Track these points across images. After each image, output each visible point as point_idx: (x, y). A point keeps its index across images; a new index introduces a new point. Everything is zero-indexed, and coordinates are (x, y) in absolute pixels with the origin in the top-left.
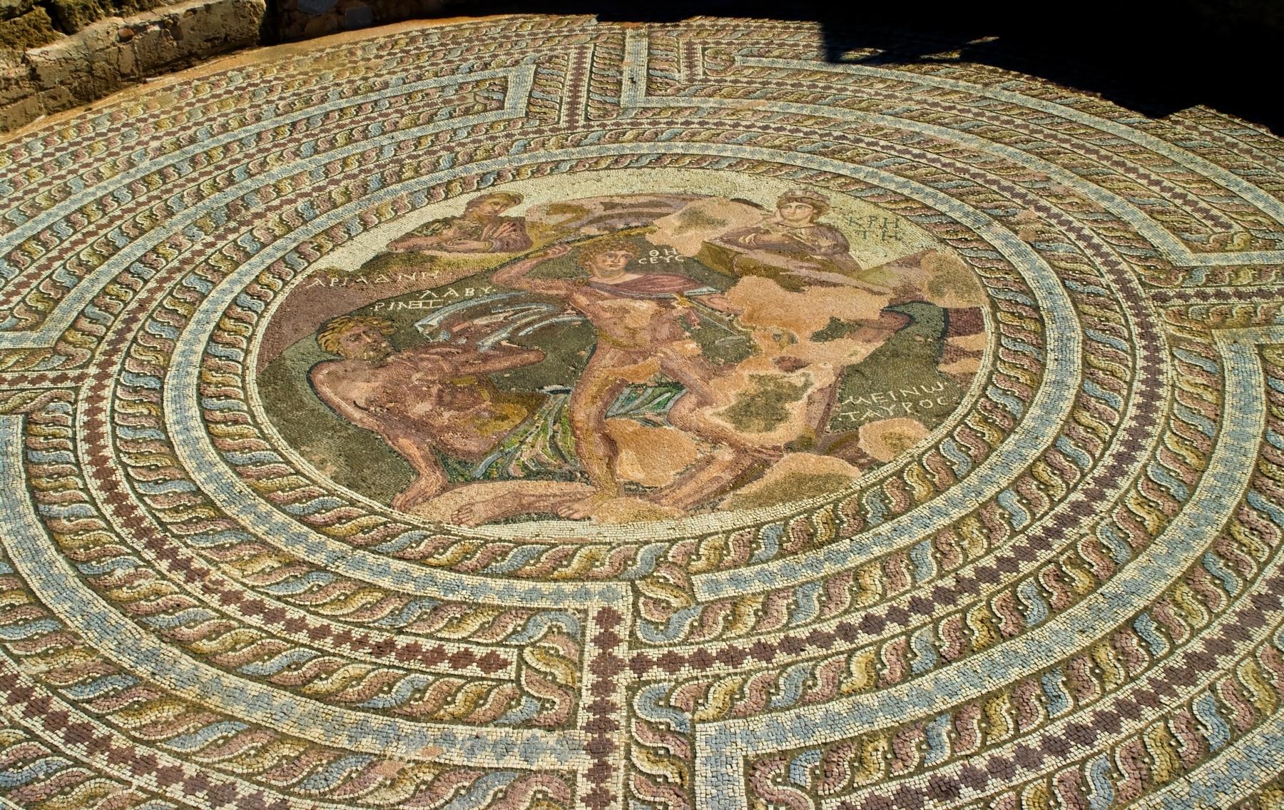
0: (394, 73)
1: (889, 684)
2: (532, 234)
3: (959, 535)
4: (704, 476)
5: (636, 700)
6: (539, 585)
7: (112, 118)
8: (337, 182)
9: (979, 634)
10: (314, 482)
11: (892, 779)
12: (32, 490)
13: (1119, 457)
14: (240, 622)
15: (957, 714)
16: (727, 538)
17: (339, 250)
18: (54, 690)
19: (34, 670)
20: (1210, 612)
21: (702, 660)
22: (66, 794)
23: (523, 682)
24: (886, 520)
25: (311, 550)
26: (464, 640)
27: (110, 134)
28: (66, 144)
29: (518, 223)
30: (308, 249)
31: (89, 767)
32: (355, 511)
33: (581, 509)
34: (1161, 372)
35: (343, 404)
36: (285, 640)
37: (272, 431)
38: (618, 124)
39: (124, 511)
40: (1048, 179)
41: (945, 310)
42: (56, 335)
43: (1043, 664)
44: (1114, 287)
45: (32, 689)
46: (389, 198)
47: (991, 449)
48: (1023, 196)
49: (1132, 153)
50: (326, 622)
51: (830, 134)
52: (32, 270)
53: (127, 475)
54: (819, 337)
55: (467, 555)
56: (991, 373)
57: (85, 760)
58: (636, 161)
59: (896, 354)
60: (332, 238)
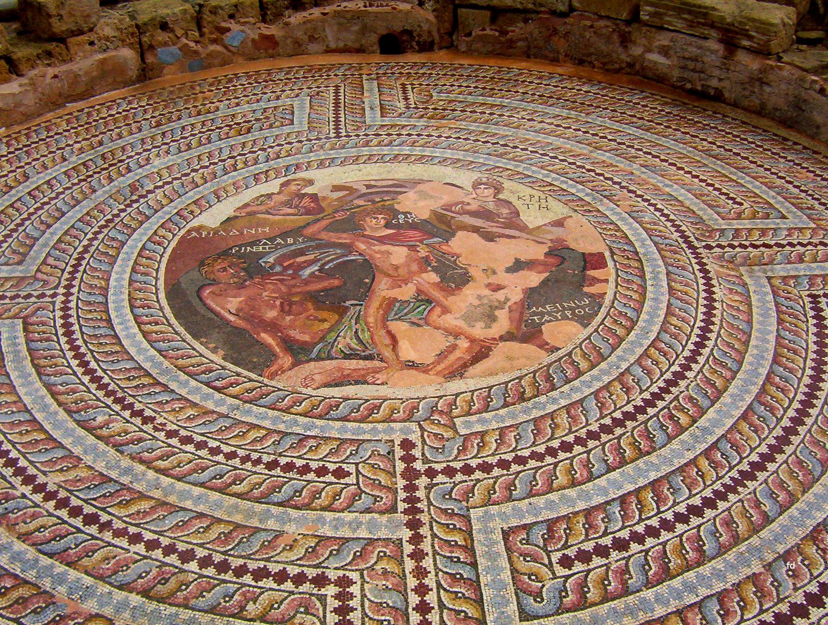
0: (222, 101)
1: (580, 484)
2: (323, 204)
3: (609, 392)
4: (452, 358)
5: (432, 494)
6: (362, 425)
7: (48, 129)
8: (196, 171)
10: (212, 362)
11: (590, 540)
12: (35, 366)
13: (696, 344)
14: (180, 449)
15: (623, 500)
16: (473, 395)
17: (204, 214)
19: (57, 480)
20: (759, 437)
21: (467, 470)
22: (89, 557)
23: (361, 485)
24: (566, 383)
26: (321, 460)
27: (48, 140)
28: (21, 146)
29: (314, 197)
30: (185, 213)
31: (103, 540)
32: (242, 379)
33: (381, 377)
34: (714, 293)
35: (222, 312)
37: (181, 329)
38: (367, 135)
39: (96, 379)
40: (632, 173)
41: (583, 254)
42: (35, 268)
44: (680, 240)
45: (57, 492)
46: (230, 181)
47: (621, 340)
48: (619, 183)
49: (680, 158)
50: (234, 449)
51: (497, 143)
52: (12, 226)
53: (94, 357)
54: (509, 270)
56: (616, 293)
57: (98, 535)
58: (382, 159)
59: (557, 281)
60: (200, 207)
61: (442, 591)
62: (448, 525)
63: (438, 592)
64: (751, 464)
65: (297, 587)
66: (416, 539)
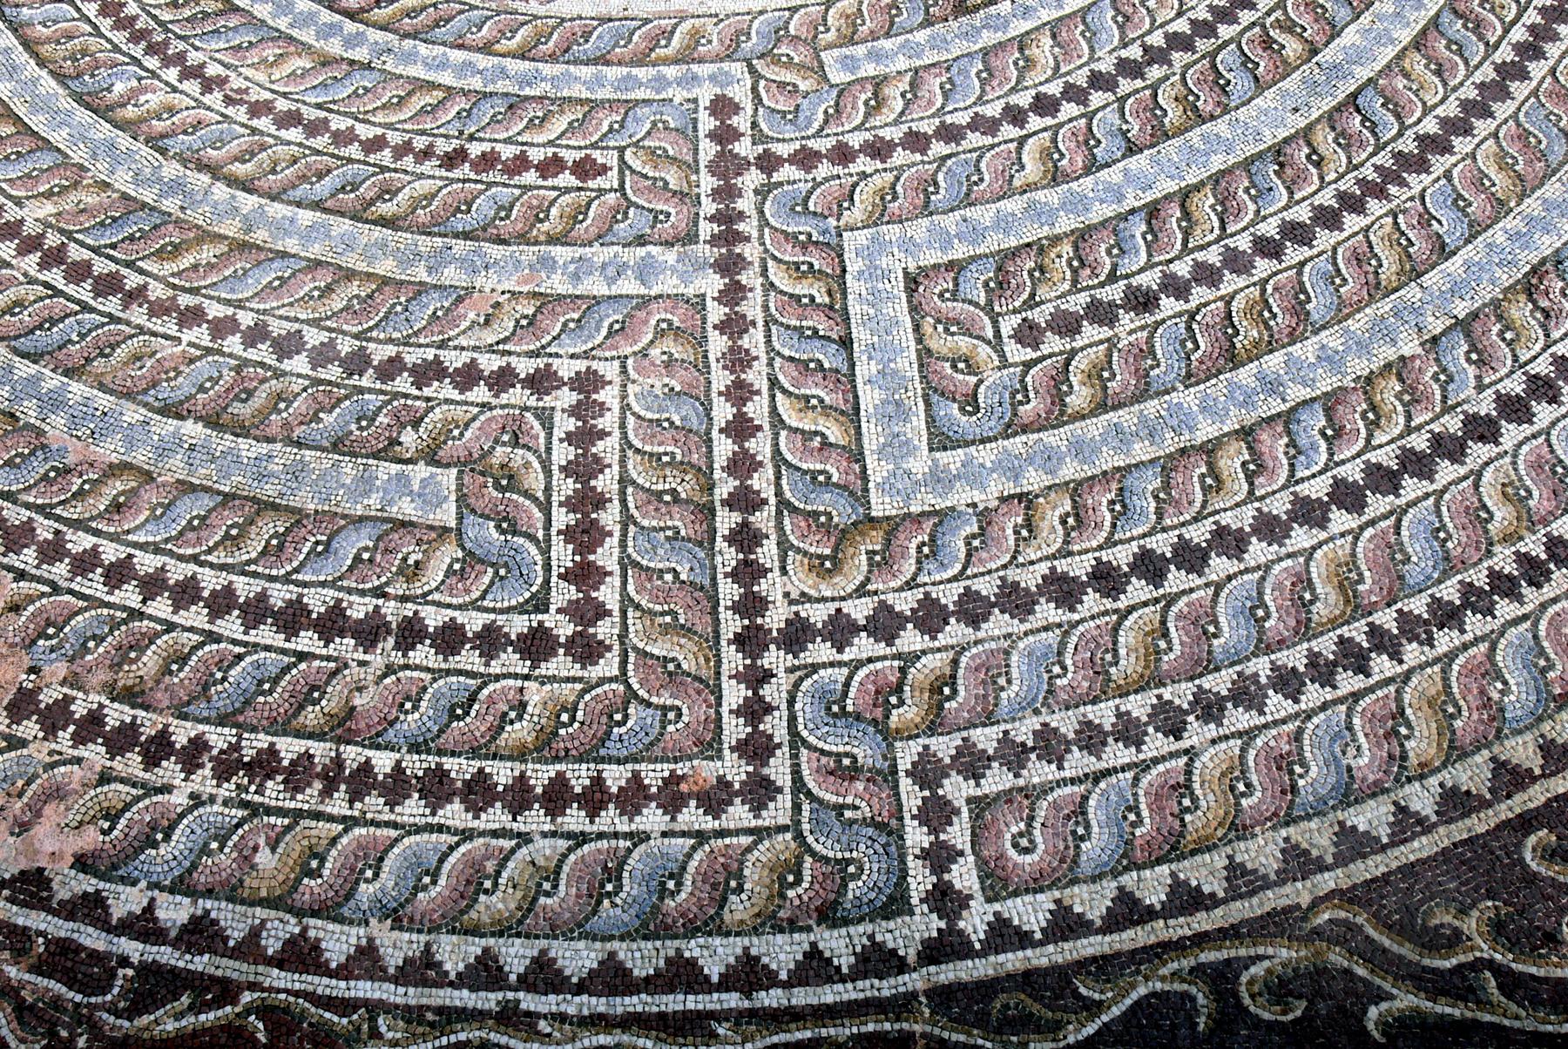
1: (1068, 178)
5: (768, 204)
6: (635, 71)
9: (1174, 114)
15: (1153, 212)
18: (69, 235)
19: (41, 214)
21: (843, 155)
25: (349, 42)
26: (551, 143)
31: (128, 323)
36: (333, 156)
43: (1252, 150)
45: (42, 235)
50: (379, 131)
55: (541, 37)
61: (779, 396)
62: (797, 266)
63: (773, 397)
64: (1421, 139)
65: (496, 396)
66: (733, 294)
